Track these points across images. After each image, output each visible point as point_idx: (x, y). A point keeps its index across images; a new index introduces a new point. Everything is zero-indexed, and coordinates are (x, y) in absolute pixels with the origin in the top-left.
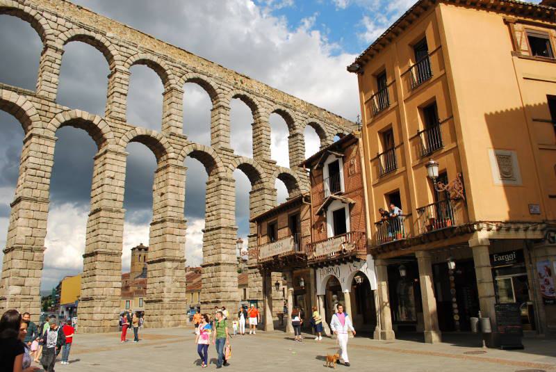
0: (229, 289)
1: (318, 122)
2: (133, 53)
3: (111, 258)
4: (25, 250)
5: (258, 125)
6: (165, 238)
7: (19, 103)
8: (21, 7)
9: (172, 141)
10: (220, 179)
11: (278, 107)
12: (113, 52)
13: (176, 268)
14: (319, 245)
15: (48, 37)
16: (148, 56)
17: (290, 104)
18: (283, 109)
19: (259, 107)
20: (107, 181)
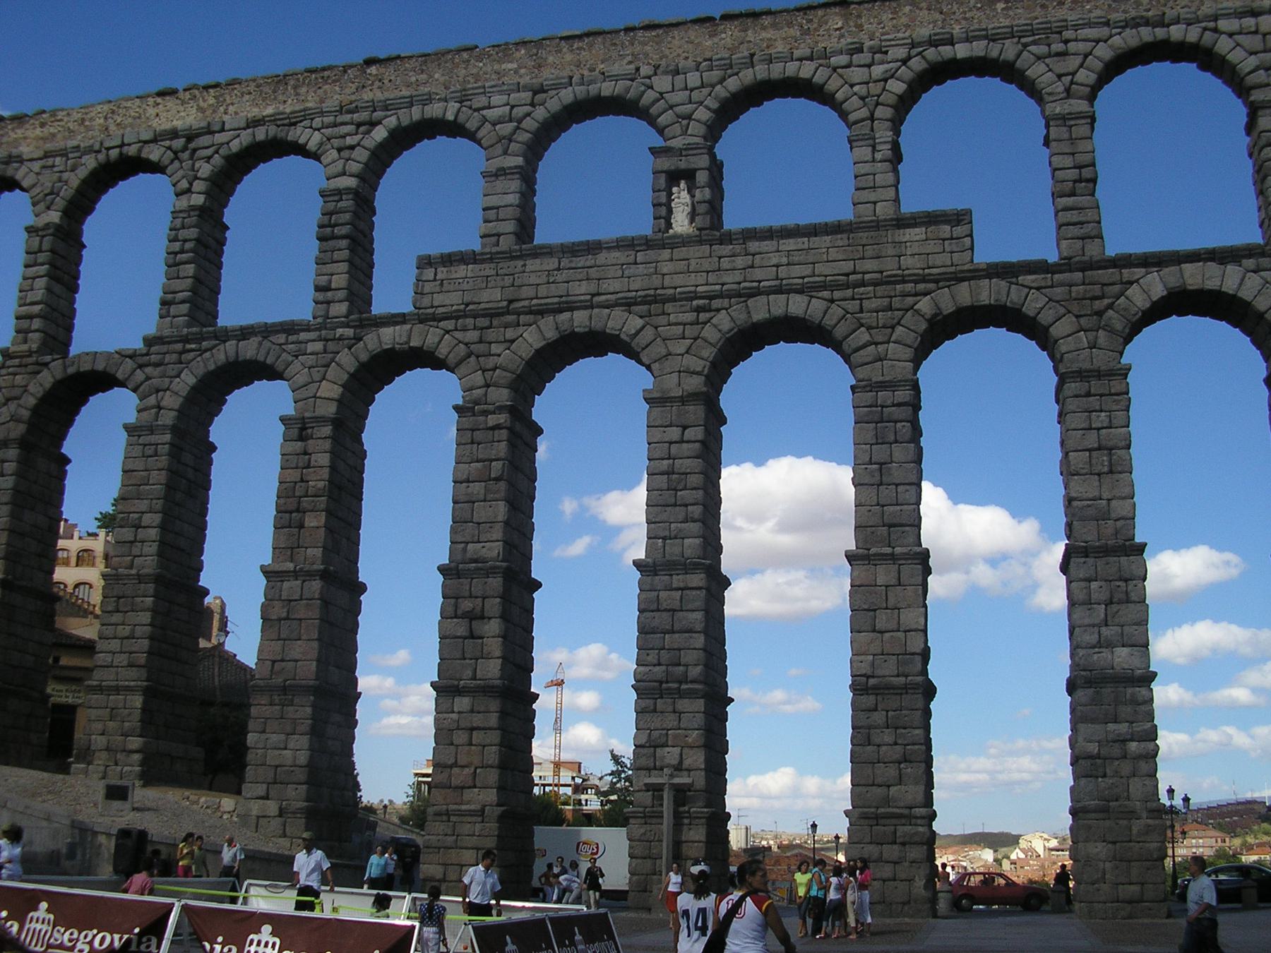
7: (1229, 286)
8: (1160, 33)
15: (1251, 80)
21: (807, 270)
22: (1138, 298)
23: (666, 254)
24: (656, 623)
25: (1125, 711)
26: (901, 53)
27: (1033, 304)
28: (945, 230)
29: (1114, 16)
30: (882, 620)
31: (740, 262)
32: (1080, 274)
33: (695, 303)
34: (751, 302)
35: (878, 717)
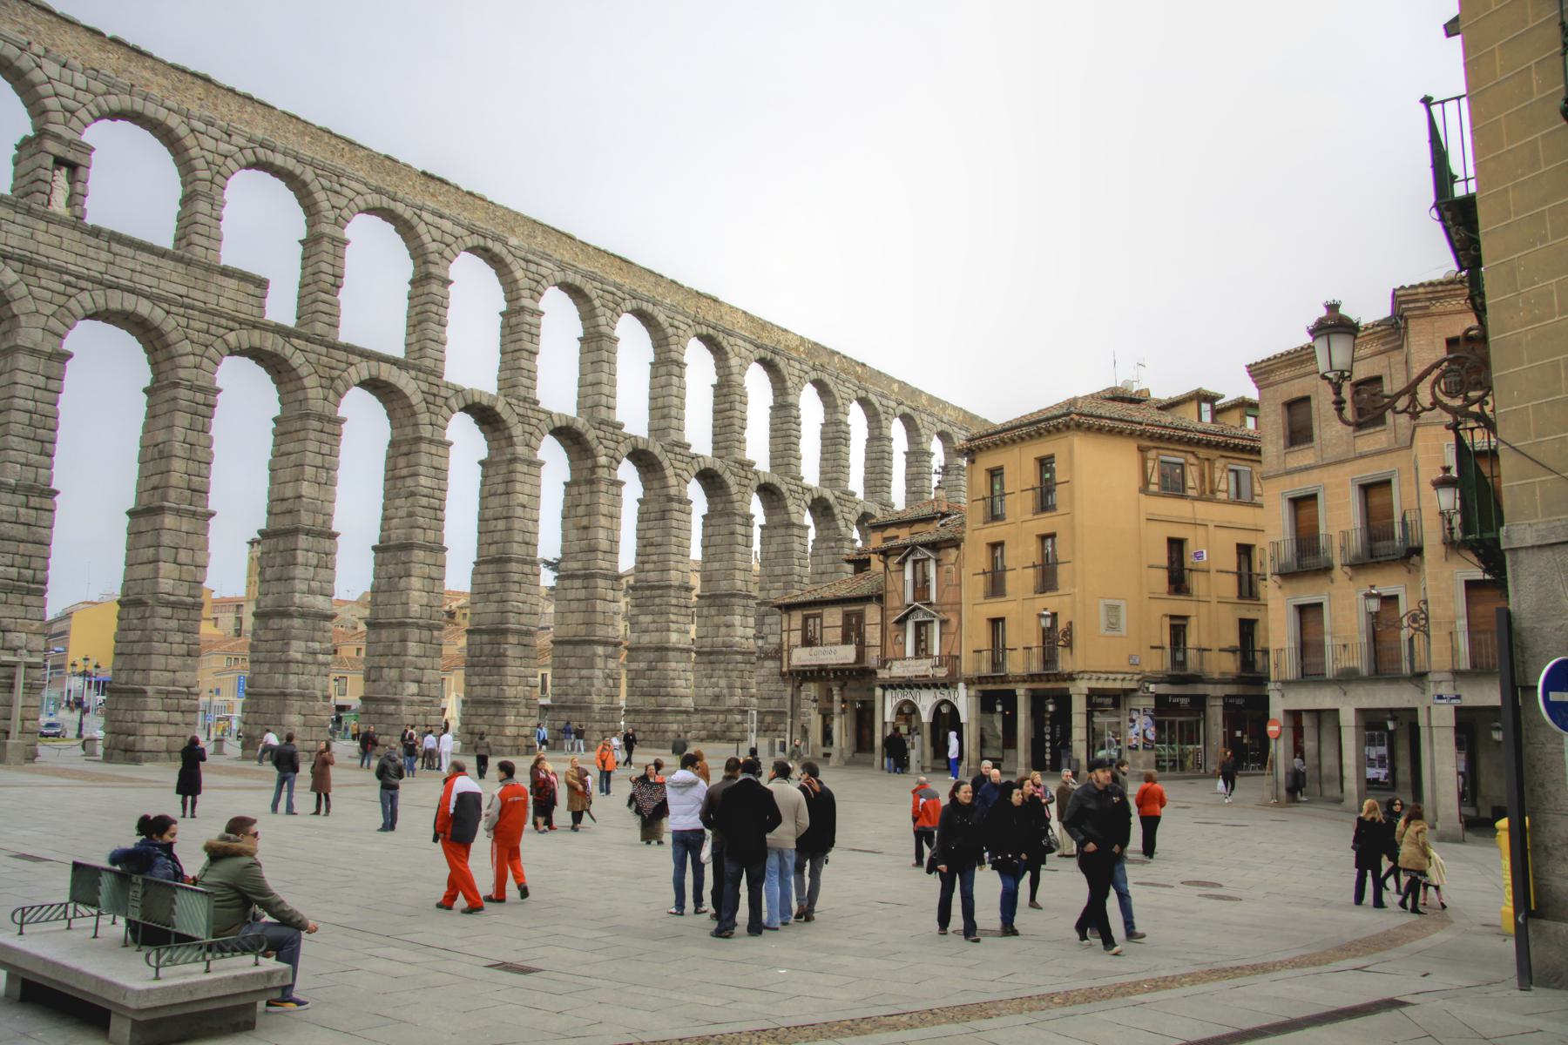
0: (682, 691)
1: (826, 379)
2: (544, 271)
3: (526, 640)
4: (419, 627)
5: (725, 391)
6: (594, 606)
8: (392, 205)
9: (601, 434)
10: (670, 499)
11: (763, 353)
12: (519, 274)
13: (607, 657)
14: (897, 664)
16: (571, 277)
17: (782, 347)
18: (769, 356)
19: (731, 355)
20: (519, 511)
21: (154, 282)
22: (353, 375)
23: (42, 225)
24: (13, 533)
25: (319, 635)
26: (242, 142)
27: (297, 360)
28: (251, 288)
29: (372, 182)
30: (183, 556)
31: (104, 256)
32: (324, 350)
33: (66, 277)
34: (109, 291)
35: (173, 624)
